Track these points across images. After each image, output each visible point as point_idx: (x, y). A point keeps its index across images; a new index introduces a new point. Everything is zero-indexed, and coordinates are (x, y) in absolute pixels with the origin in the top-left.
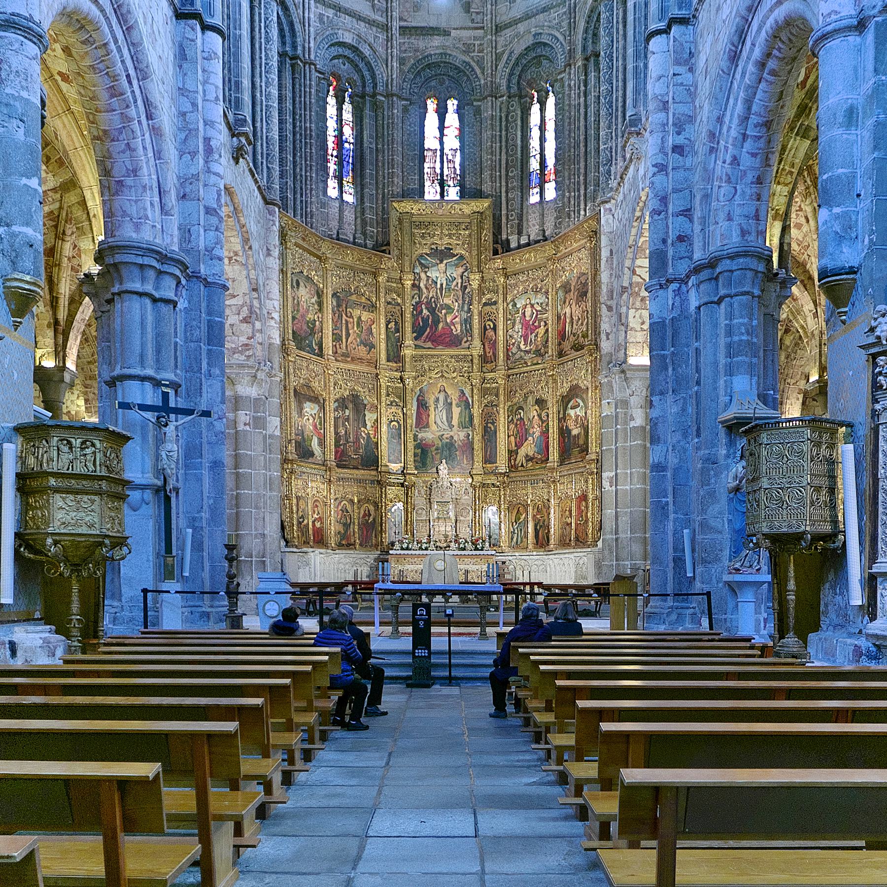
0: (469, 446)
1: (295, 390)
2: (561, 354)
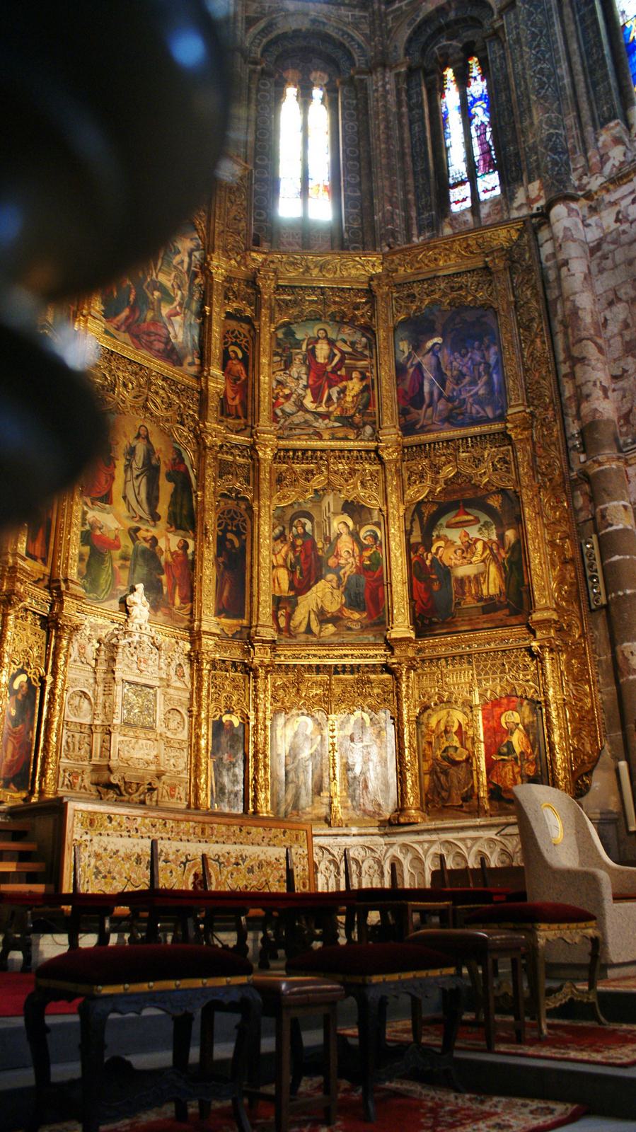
0: (189, 567)
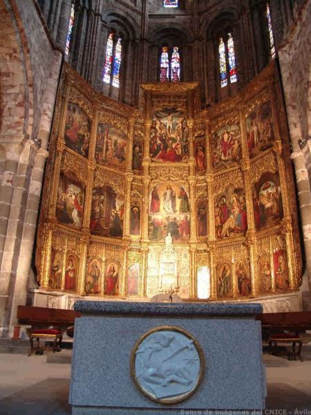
0: (188, 223)
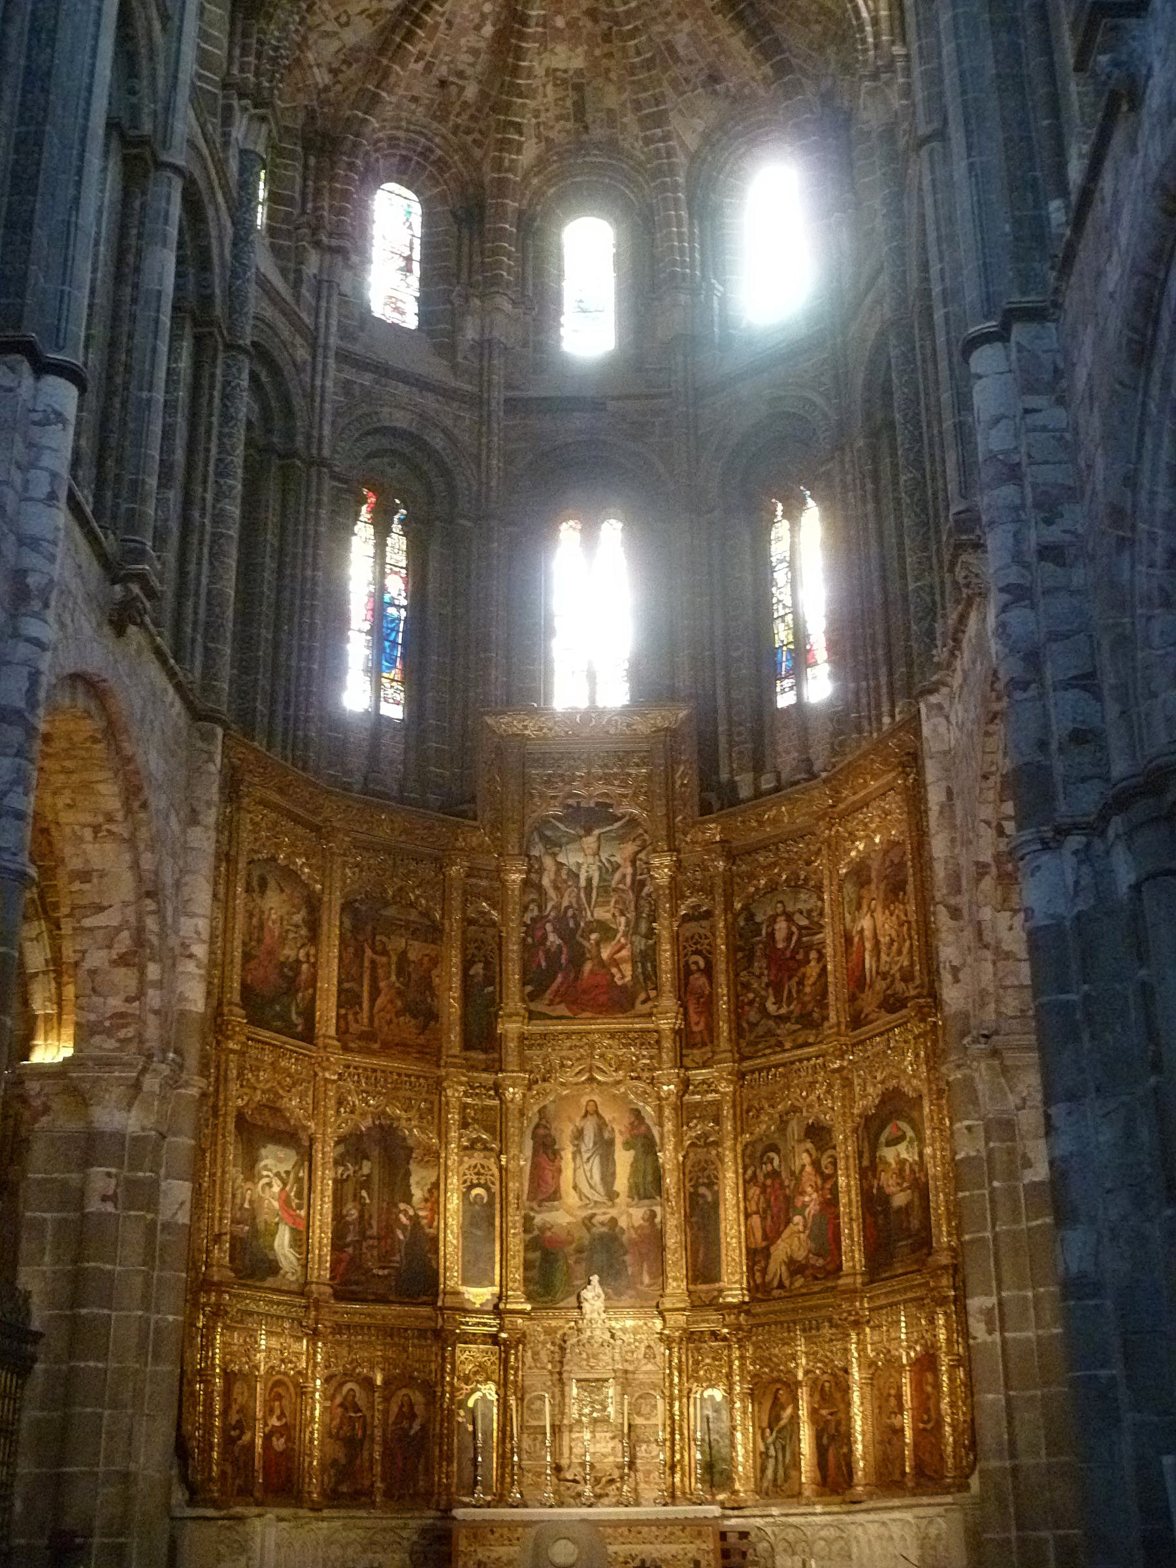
0: (654, 1238)
1: (240, 1118)
2: (857, 1021)
